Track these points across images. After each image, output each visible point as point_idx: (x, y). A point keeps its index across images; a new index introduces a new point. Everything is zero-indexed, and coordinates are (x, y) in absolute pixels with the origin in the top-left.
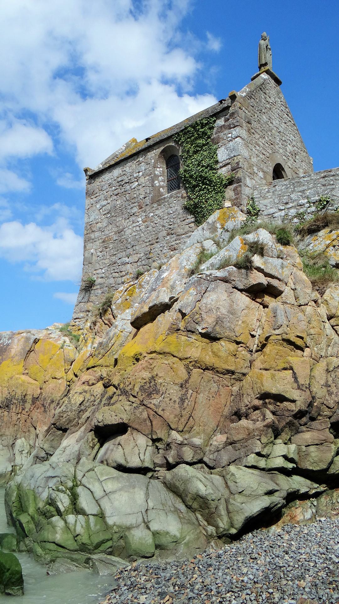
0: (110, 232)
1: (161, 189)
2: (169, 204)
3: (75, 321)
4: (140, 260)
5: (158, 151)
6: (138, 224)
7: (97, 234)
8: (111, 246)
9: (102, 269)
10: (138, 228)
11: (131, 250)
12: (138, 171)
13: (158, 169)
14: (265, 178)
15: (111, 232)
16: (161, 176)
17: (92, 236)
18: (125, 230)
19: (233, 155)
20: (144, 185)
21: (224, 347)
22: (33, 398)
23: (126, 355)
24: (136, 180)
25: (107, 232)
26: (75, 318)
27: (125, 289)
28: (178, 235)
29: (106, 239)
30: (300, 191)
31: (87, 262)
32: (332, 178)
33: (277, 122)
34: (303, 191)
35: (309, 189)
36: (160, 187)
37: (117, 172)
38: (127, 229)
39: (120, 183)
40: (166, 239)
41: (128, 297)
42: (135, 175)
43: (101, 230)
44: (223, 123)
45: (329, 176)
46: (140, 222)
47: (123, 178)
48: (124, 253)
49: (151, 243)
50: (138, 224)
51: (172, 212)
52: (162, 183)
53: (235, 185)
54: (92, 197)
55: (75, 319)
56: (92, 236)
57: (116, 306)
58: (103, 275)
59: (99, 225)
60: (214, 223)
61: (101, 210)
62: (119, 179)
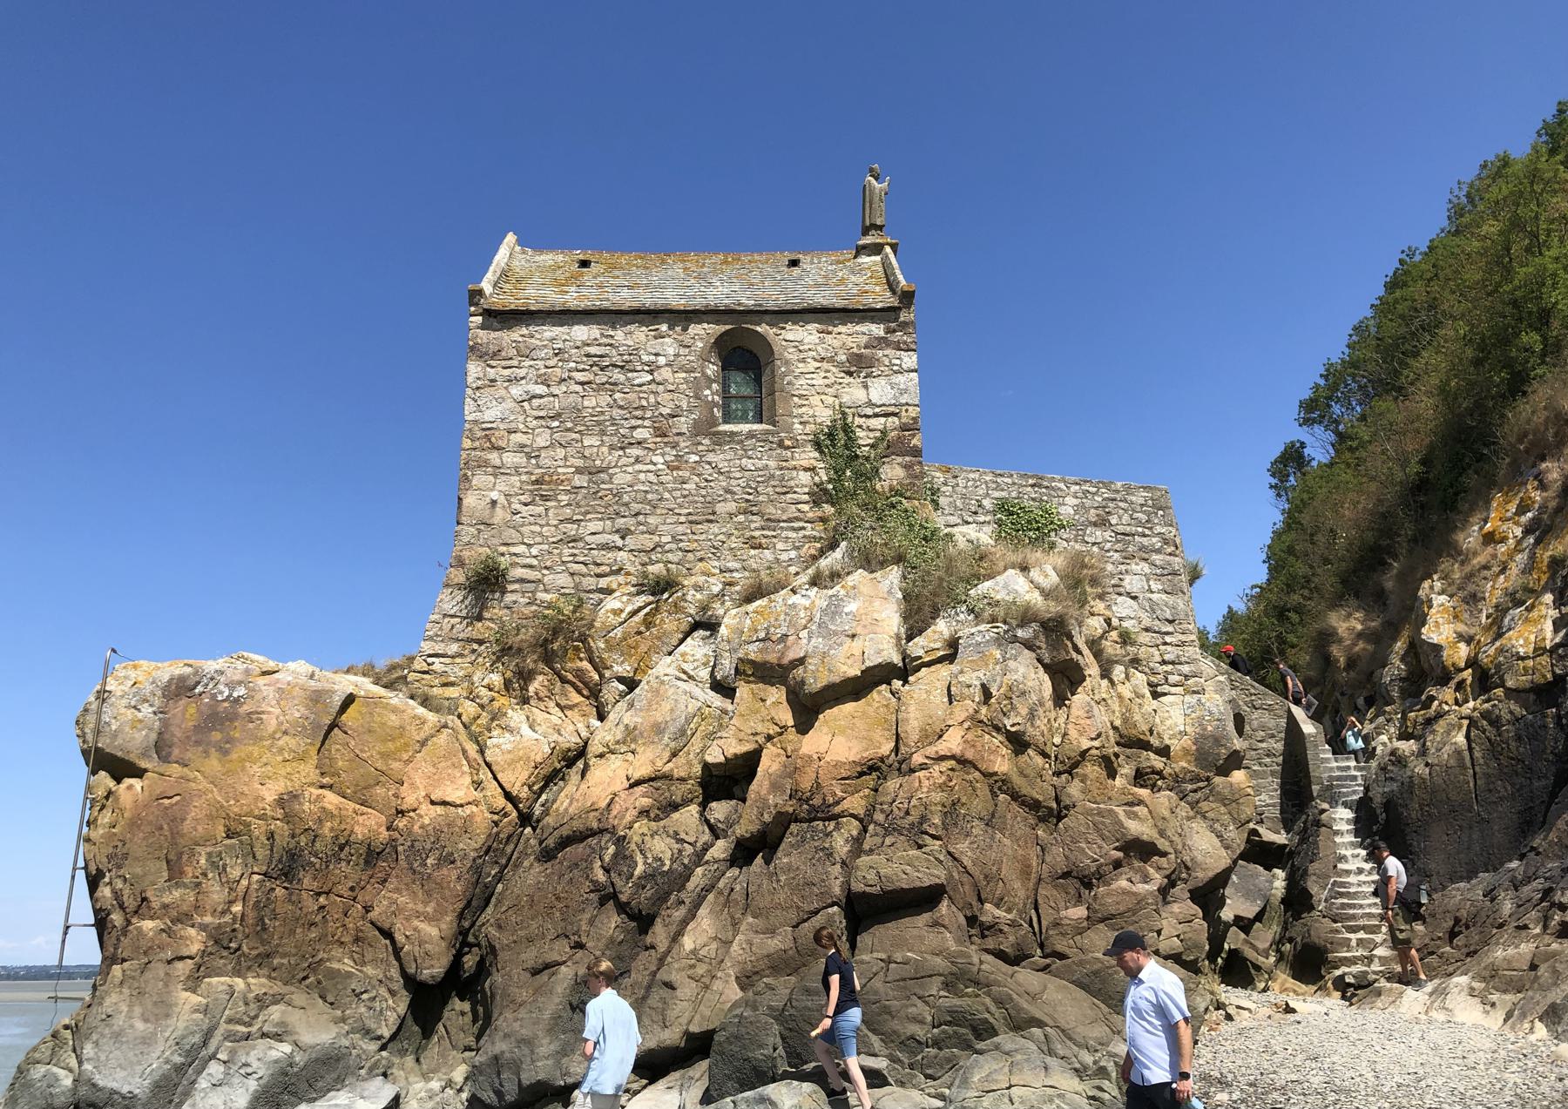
0: (560, 463)
1: (715, 410)
2: (745, 450)
3: (430, 660)
5: (715, 329)
7: (510, 459)
8: (564, 498)
9: (530, 546)
10: (652, 477)
11: (632, 521)
16: (715, 381)
17: (494, 457)
18: (611, 471)
19: (904, 401)
20: (671, 387)
21: (1033, 759)
22: (370, 851)
23: (828, 759)
24: (646, 368)
25: (548, 462)
26: (432, 652)
27: (629, 608)
28: (769, 520)
32: (1044, 490)
36: (715, 404)
37: (581, 332)
38: (617, 470)
40: (735, 519)
41: (642, 629)
42: (645, 358)
44: (882, 333)
45: (1040, 486)
46: (660, 466)
47: (606, 350)
48: (608, 522)
49: (690, 518)
51: (753, 468)
53: (907, 459)
54: (493, 363)
55: (430, 656)
57: (607, 642)
58: (535, 562)
59: (518, 438)
61: (525, 404)
62: (593, 350)
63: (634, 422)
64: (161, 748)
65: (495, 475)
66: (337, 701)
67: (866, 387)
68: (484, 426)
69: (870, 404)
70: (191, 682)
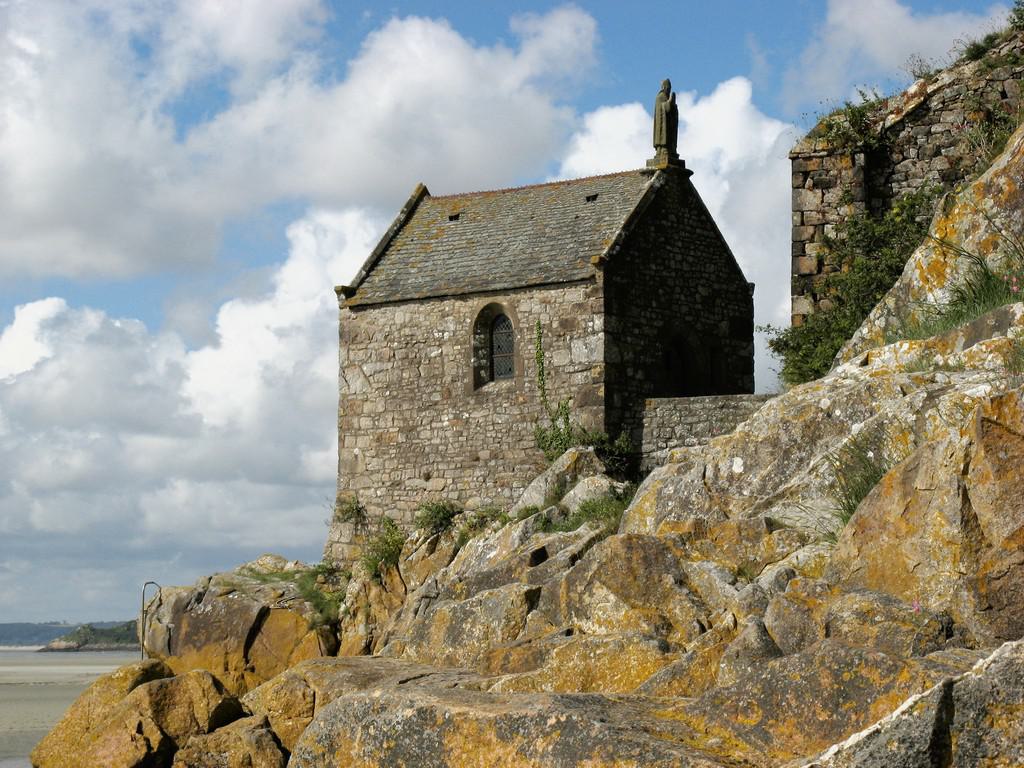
1: (482, 372)
4: (446, 489)
6: (439, 425)
7: (365, 422)
9: (376, 489)
12: (441, 328)
13: (477, 336)
15: (390, 425)
16: (482, 348)
17: (355, 420)
20: (452, 358)
29: (384, 436)
30: (687, 424)
33: (679, 257)
34: (691, 424)
35: (699, 422)
37: (400, 314)
39: (409, 339)
43: (375, 416)
50: (439, 425)
53: (595, 408)
59: (367, 407)
60: (563, 474)
62: (407, 331)
63: (430, 389)
64: (170, 645)
65: (356, 436)
66: (255, 612)
67: (570, 348)
68: (350, 398)
69: (572, 363)
70: (185, 603)
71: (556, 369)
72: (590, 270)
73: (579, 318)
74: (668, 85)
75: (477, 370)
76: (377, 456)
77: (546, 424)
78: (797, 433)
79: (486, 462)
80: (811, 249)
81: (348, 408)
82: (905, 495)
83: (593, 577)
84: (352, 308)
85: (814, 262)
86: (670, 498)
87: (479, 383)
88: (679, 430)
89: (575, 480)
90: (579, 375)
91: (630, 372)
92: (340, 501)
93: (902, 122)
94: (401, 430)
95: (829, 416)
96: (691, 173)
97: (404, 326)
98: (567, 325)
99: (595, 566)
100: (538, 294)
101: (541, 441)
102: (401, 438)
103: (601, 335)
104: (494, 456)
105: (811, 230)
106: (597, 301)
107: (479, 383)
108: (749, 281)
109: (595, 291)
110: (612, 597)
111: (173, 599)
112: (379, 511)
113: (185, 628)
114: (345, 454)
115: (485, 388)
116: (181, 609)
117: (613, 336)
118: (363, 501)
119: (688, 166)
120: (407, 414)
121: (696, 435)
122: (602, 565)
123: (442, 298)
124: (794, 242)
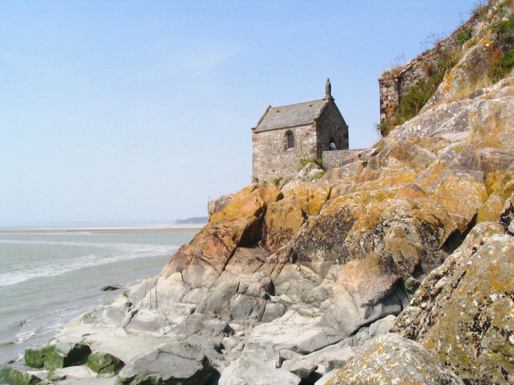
5: (285, 130)
7: (259, 159)
14: (326, 146)
15: (265, 159)
31: (255, 169)
34: (337, 157)
37: (267, 134)
42: (276, 138)
43: (261, 157)
52: (287, 144)
56: (256, 159)
59: (259, 155)
62: (269, 137)
67: (308, 140)
69: (309, 143)
71: (305, 144)
72: (312, 121)
73: (310, 132)
74: (328, 80)
75: (285, 146)
76: (262, 166)
77: (302, 158)
78: (437, 117)
79: (288, 167)
80: (385, 103)
81: (255, 156)
82: (497, 120)
83: (388, 155)
84: (255, 133)
85: (386, 105)
86: (399, 137)
87: (286, 149)
88: (334, 158)
89: (310, 170)
90: (311, 146)
91: (322, 145)
92: (253, 177)
93: (406, 71)
94: (267, 160)
95: (447, 112)
96: (334, 99)
97: (268, 136)
98: (307, 134)
99: (389, 151)
100: (300, 128)
101: (301, 161)
102: (268, 162)
103: (316, 136)
104: (290, 165)
105: (384, 98)
106: (314, 128)
107: (286, 149)
108: (347, 125)
109: (314, 126)
110: (395, 160)
111: (215, 201)
112: (262, 179)
113: (218, 207)
114: (254, 166)
115: (288, 150)
116: (217, 203)
117: (319, 137)
118: (258, 177)
119: (334, 98)
120: (269, 157)
121: (339, 159)
122: (391, 151)
123: (276, 129)
124: (380, 101)
